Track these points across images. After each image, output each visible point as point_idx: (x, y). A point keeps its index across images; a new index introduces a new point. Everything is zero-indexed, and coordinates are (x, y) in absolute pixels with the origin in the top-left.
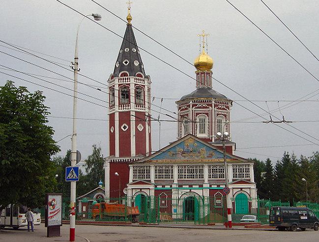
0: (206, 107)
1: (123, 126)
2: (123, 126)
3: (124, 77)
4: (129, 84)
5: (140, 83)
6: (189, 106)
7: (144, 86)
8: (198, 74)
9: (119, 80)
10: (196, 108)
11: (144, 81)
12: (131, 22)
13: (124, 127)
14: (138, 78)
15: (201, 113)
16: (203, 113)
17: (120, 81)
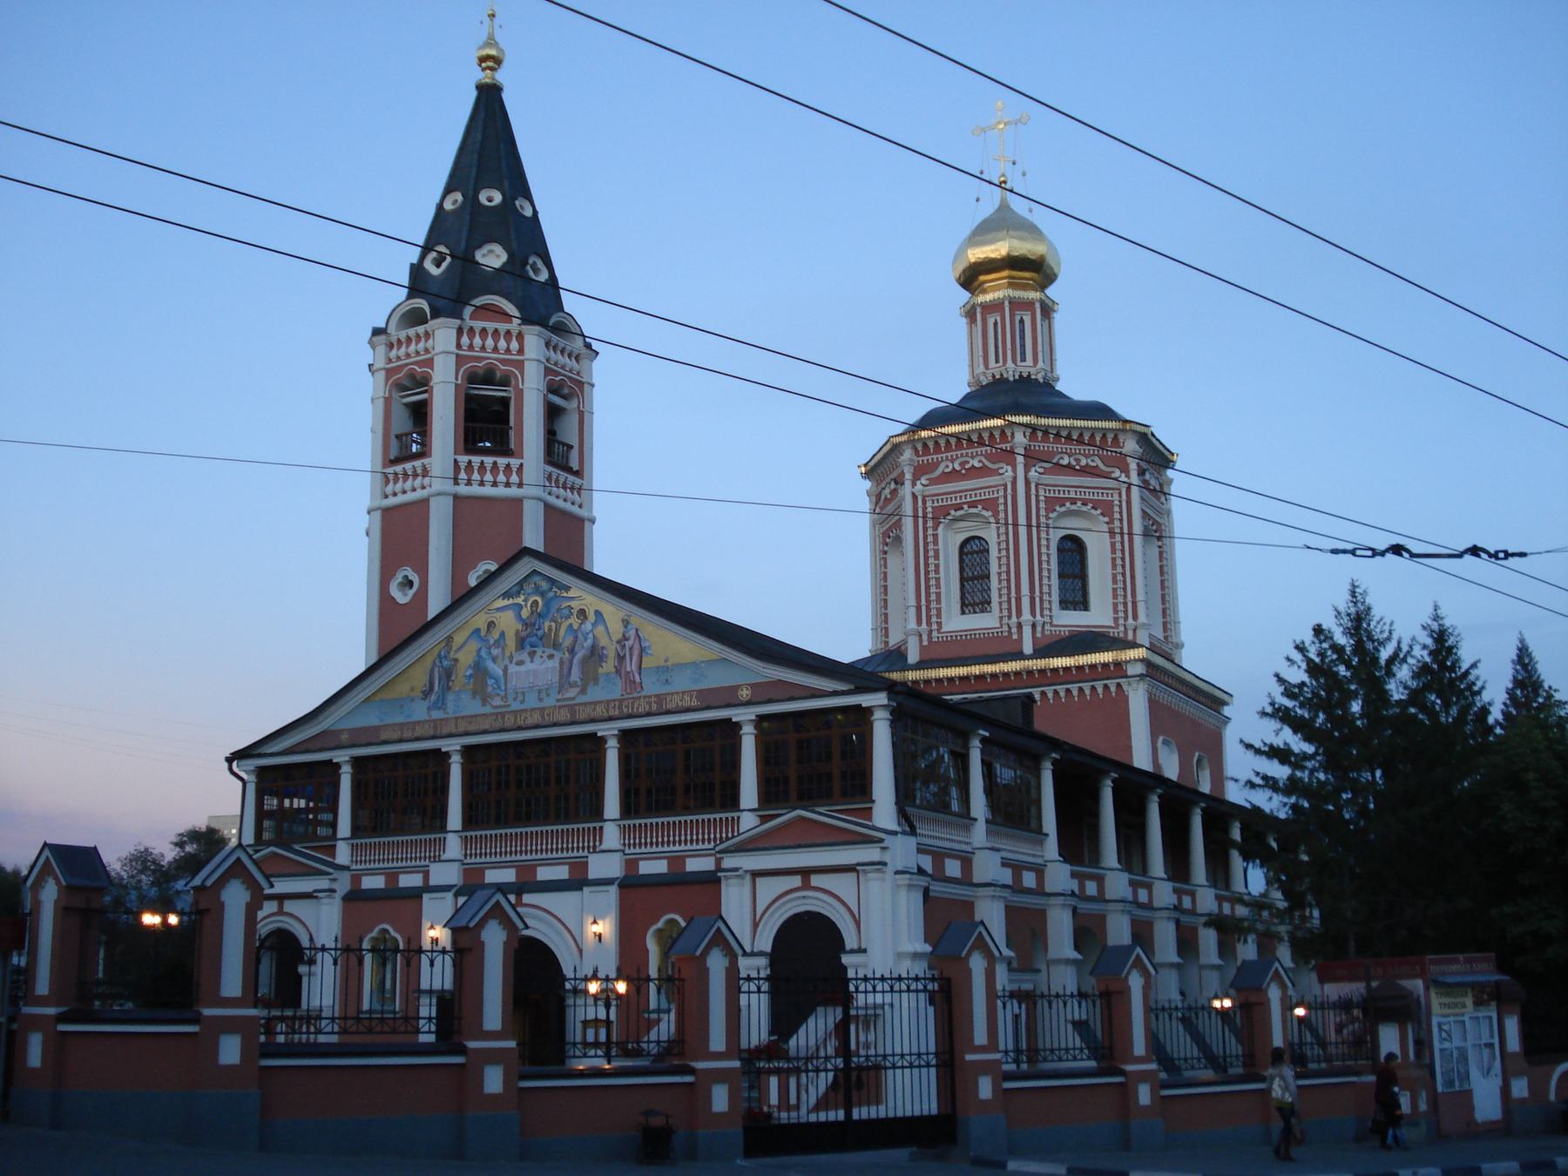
0: (983, 472)
1: (399, 578)
2: (399, 578)
3: (412, 332)
4: (429, 363)
5: (489, 351)
6: (899, 481)
7: (520, 365)
8: (970, 314)
9: (391, 346)
10: (933, 482)
11: (520, 337)
12: (501, 77)
13: (411, 584)
14: (478, 325)
15: (959, 507)
16: (972, 505)
17: (393, 353)
